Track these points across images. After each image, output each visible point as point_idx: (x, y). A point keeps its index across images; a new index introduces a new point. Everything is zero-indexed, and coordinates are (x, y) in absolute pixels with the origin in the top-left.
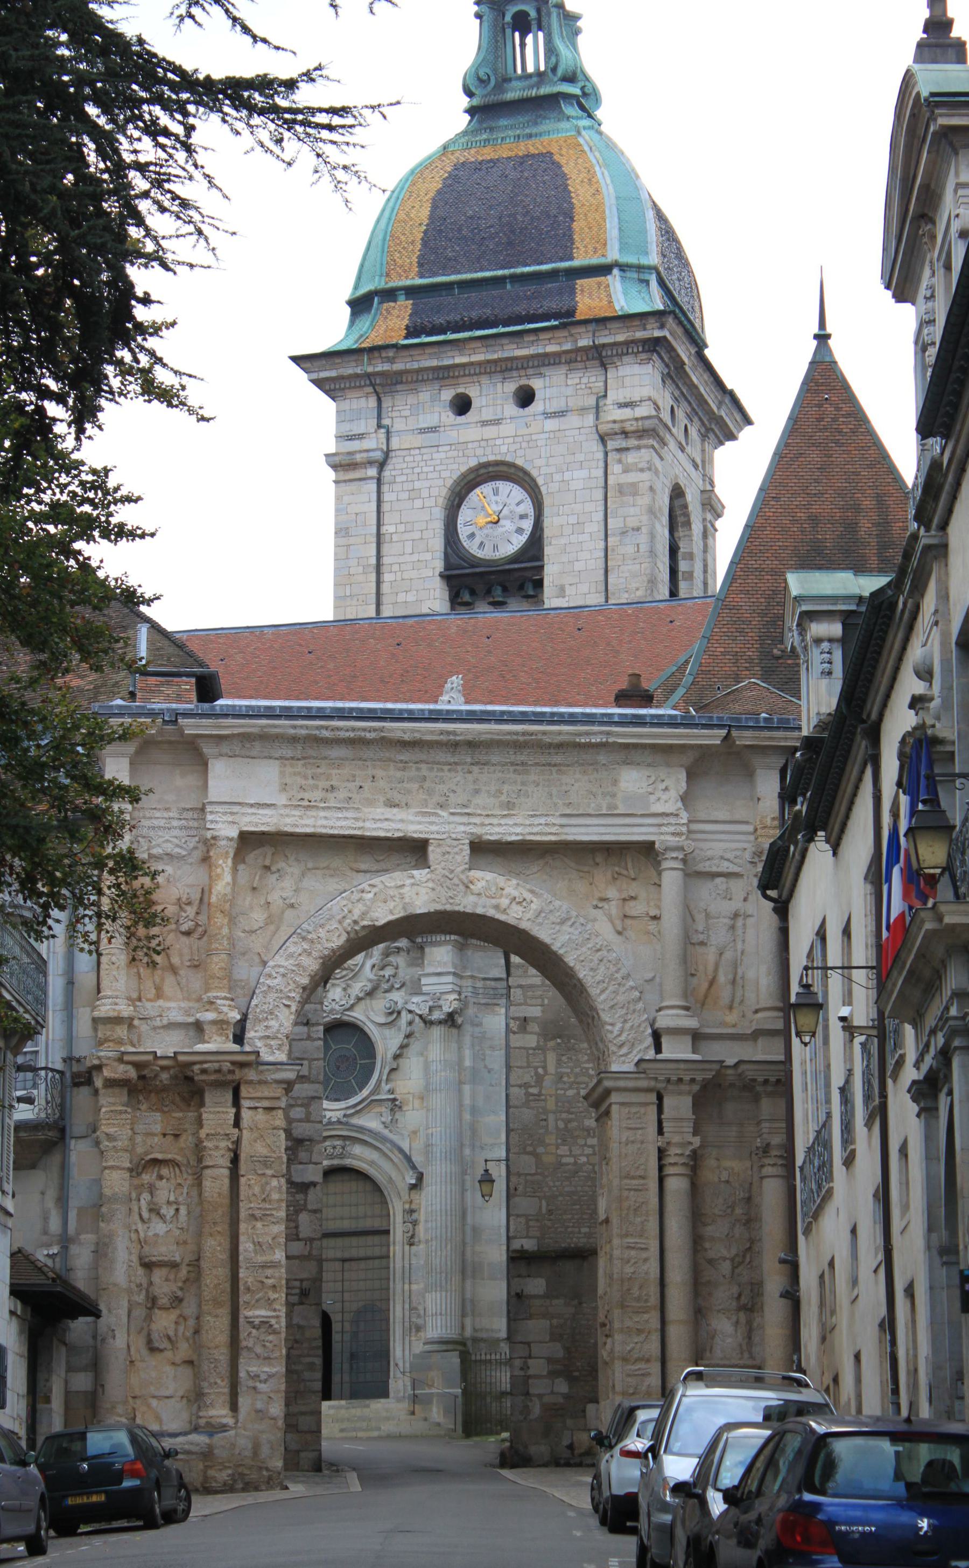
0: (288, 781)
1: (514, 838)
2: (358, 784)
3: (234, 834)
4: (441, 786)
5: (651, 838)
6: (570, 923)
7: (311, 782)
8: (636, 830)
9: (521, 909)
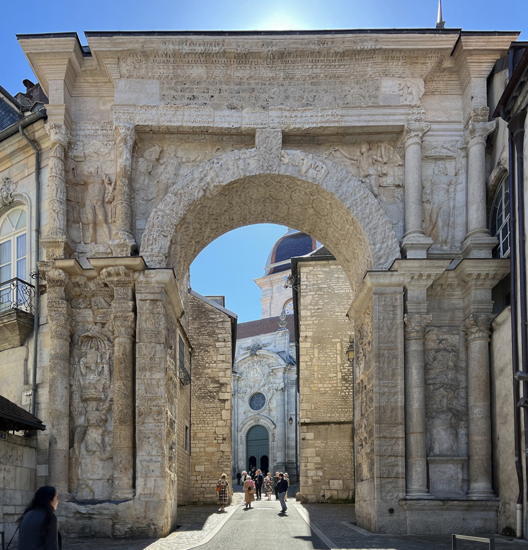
0: (165, 93)
1: (311, 126)
2: (210, 94)
3: (132, 127)
4: (264, 94)
5: (401, 123)
6: (347, 180)
7: (181, 94)
8: (391, 118)
9: (315, 172)
